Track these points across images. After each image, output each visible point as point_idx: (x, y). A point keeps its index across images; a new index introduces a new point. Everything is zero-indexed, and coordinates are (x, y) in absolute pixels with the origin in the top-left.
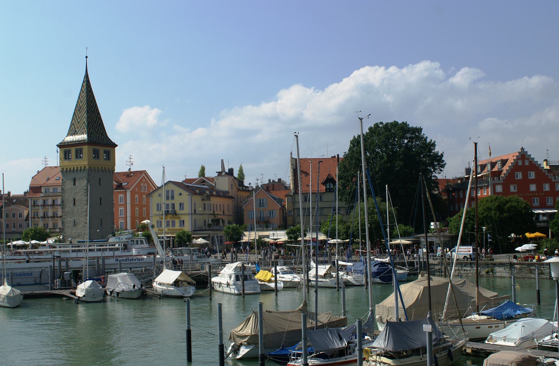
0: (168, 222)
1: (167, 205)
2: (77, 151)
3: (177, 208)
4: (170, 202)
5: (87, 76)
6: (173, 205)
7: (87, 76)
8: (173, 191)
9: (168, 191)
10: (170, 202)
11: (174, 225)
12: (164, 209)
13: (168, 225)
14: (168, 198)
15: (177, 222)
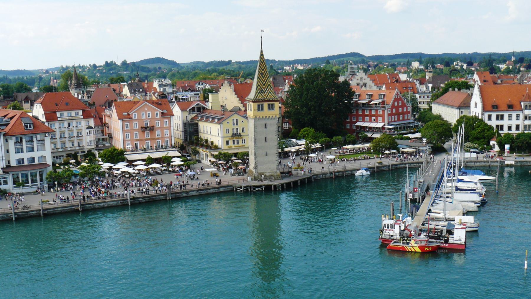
0: (234, 141)
1: (233, 129)
2: (269, 105)
3: (240, 131)
4: (235, 127)
5: (262, 51)
6: (237, 129)
7: (262, 51)
8: (237, 120)
9: (233, 120)
10: (235, 127)
11: (238, 143)
12: (231, 132)
13: (234, 143)
14: (234, 124)
15: (240, 141)
